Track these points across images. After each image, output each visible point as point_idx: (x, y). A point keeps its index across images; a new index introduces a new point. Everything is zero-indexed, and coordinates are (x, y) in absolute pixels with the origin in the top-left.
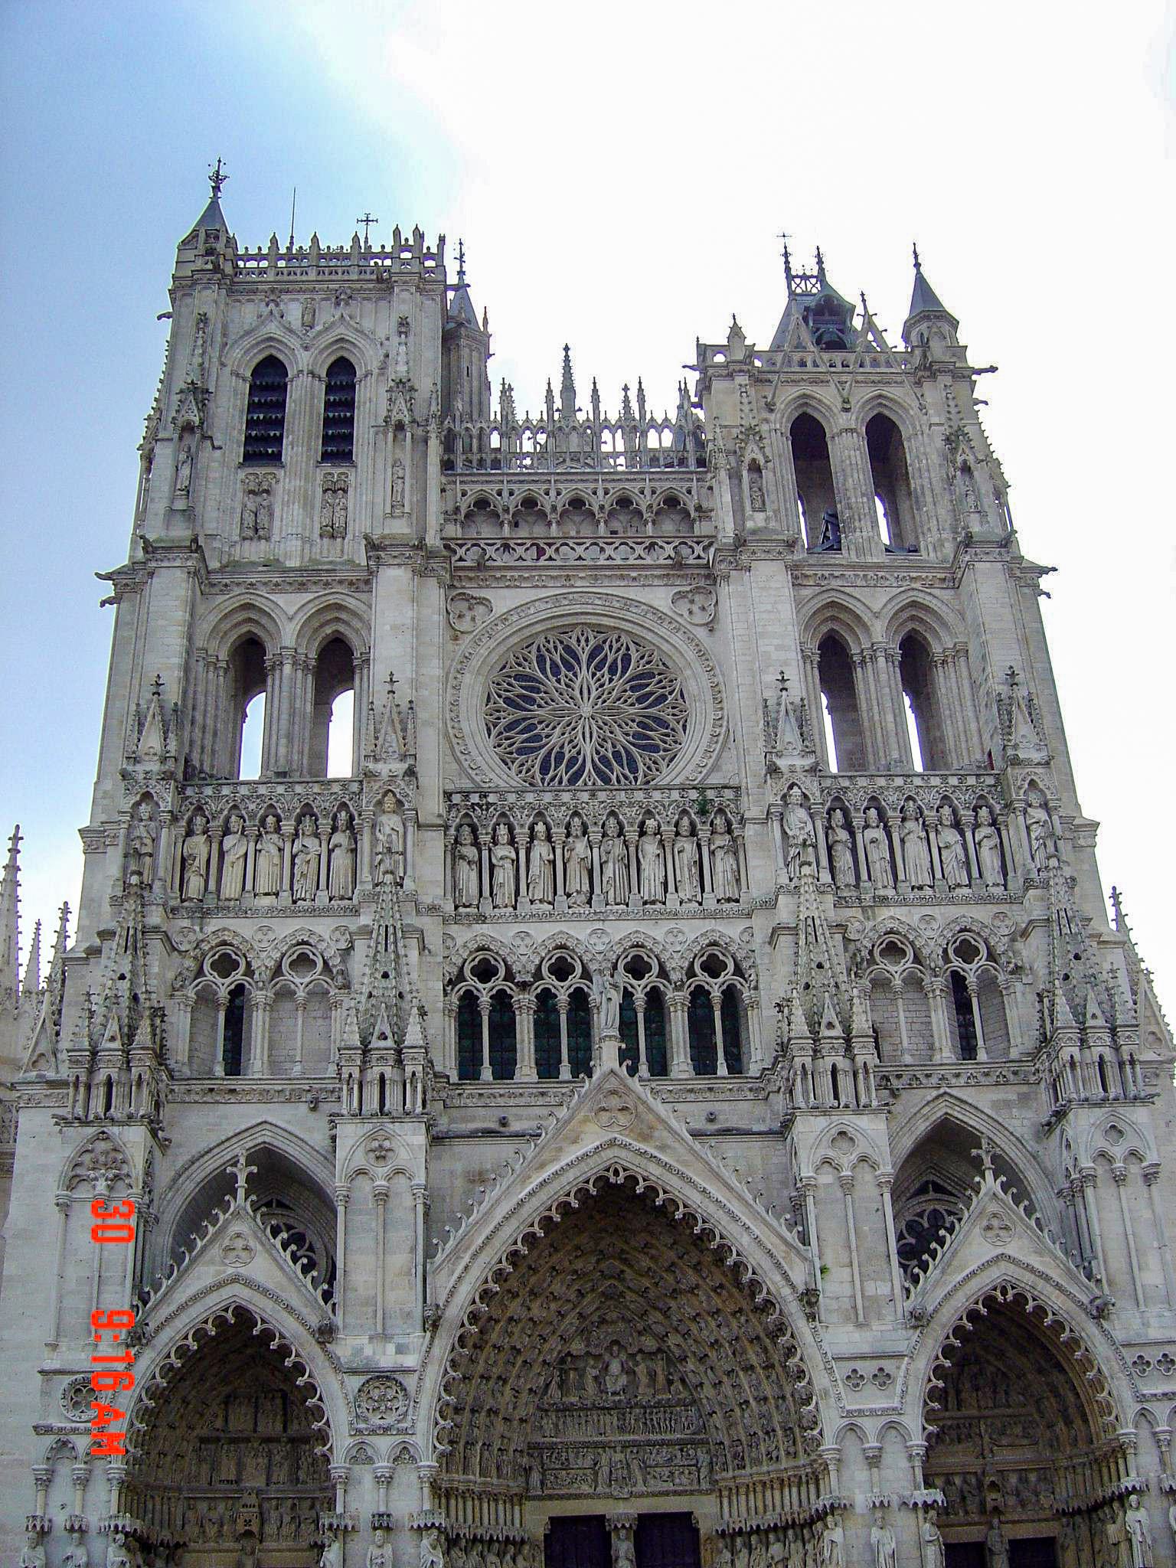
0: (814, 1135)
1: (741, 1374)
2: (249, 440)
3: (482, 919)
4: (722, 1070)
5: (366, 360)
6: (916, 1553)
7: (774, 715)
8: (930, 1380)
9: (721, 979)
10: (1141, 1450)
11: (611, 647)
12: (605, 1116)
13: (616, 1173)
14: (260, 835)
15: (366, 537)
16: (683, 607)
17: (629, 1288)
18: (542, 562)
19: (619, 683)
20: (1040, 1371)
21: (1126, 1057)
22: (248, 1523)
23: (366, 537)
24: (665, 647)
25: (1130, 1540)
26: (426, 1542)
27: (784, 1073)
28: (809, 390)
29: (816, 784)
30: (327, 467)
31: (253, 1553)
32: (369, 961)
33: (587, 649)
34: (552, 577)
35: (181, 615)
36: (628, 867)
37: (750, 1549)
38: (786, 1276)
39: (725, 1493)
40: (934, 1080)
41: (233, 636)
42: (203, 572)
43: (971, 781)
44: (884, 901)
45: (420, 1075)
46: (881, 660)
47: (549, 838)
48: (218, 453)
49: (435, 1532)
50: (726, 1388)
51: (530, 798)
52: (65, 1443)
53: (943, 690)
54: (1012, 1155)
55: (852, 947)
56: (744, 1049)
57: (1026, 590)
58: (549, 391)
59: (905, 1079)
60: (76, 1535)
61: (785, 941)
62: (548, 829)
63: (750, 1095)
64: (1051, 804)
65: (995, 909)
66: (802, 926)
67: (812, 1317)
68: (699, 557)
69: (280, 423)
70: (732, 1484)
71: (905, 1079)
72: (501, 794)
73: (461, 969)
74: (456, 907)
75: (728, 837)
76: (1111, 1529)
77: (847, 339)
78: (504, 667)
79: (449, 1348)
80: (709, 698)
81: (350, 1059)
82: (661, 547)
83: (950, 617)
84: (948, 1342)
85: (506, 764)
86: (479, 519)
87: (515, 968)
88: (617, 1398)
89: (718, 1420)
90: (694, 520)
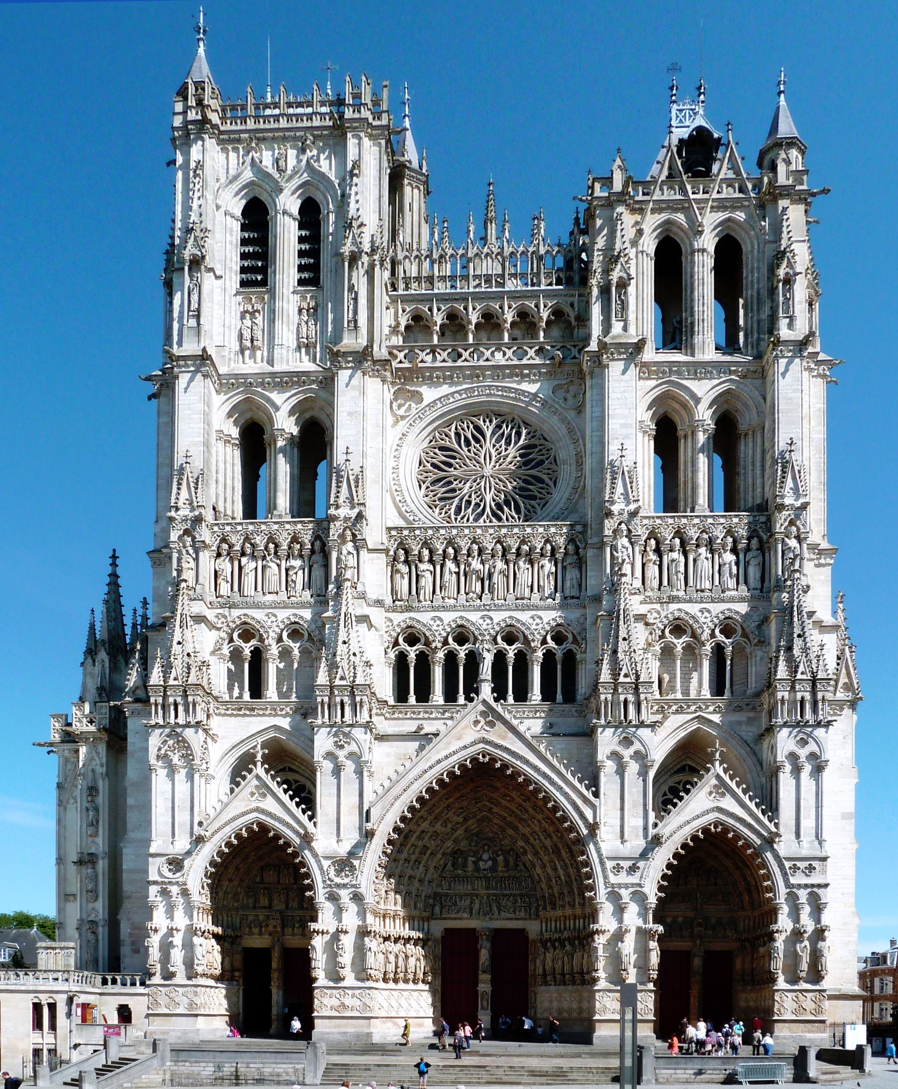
3: (409, 609)
14: (265, 556)
18: (459, 363)
29: (638, 522)
33: (491, 428)
36: (508, 577)
40: (693, 708)
44: (673, 599)
51: (442, 532)
52: (165, 889)
53: (742, 455)
59: (674, 708)
62: (456, 551)
68: (574, 357)
72: (426, 529)
74: (394, 601)
75: (575, 557)
76: (762, 950)
78: (431, 441)
80: (573, 462)
85: (431, 508)
86: (416, 330)
87: (431, 639)
90: (574, 328)
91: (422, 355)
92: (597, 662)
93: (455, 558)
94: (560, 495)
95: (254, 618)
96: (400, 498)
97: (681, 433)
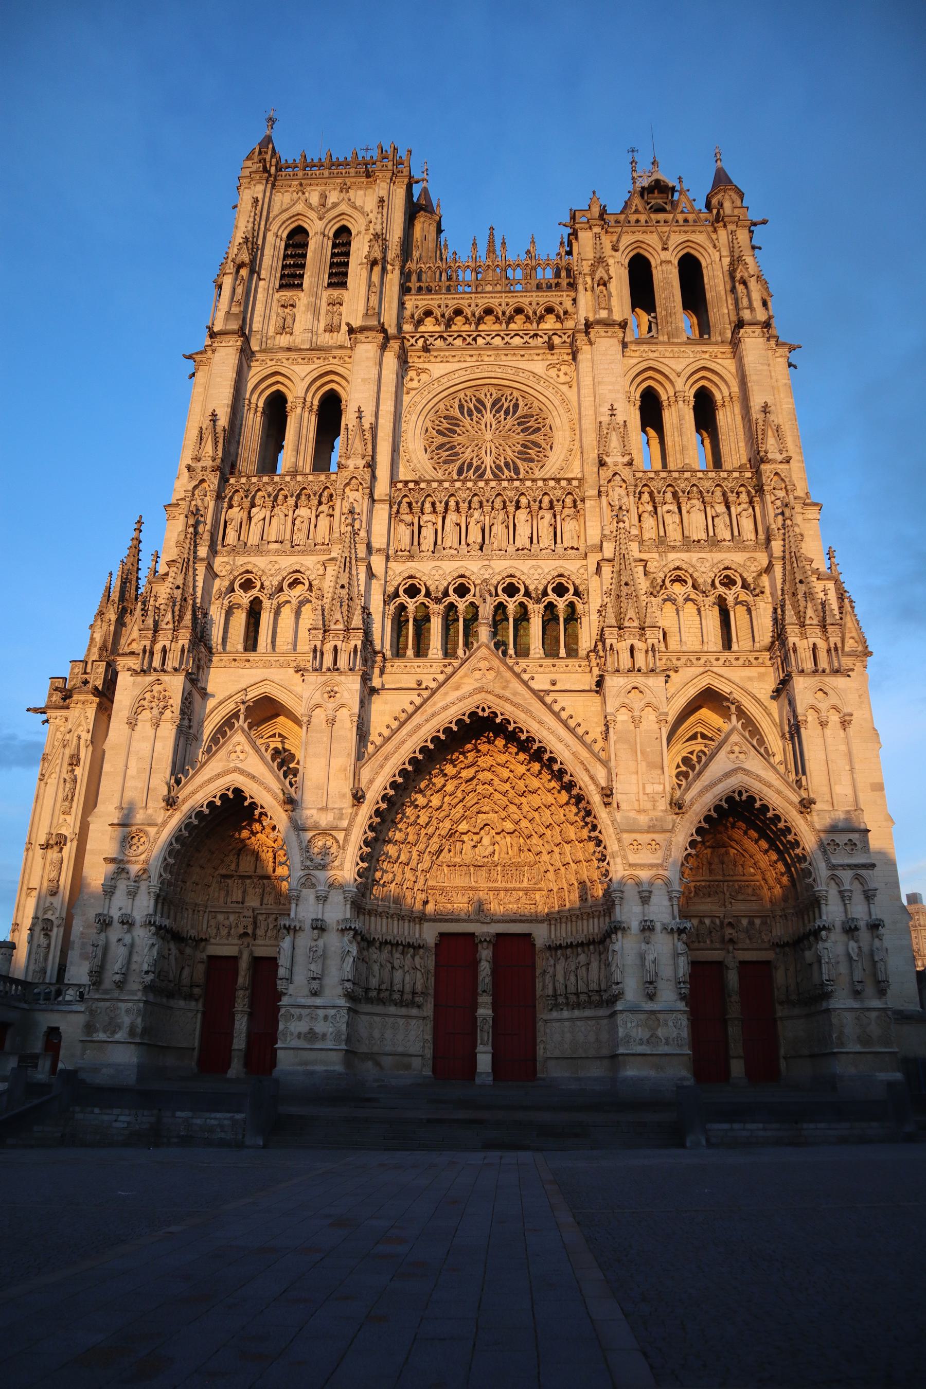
0: (616, 689)
1: (565, 845)
2: (283, 277)
3: (411, 557)
4: (563, 653)
5: (356, 226)
6: (671, 962)
7: (605, 432)
8: (686, 849)
9: (565, 598)
10: (829, 903)
11: (506, 399)
12: (477, 674)
13: (483, 710)
14: (273, 507)
15: (348, 324)
16: (553, 372)
17: (495, 790)
19: (510, 421)
20: (766, 852)
21: (832, 646)
22: (245, 927)
23: (348, 324)
24: (541, 398)
25: (820, 962)
26: (346, 939)
27: (601, 653)
28: (640, 237)
30: (331, 291)
31: (248, 946)
32: (333, 579)
34: (471, 356)
35: (231, 375)
36: (507, 527)
37: (567, 958)
38: (592, 777)
39: (553, 922)
40: (702, 661)
41: (268, 392)
42: (249, 352)
43: (736, 475)
45: (359, 647)
46: (681, 403)
47: (458, 510)
48: (262, 283)
49: (352, 933)
50: (556, 855)
52: (123, 869)
54: (752, 711)
55: (652, 576)
56: (580, 645)
57: (780, 359)
58: (475, 244)
59: (683, 661)
60: (125, 926)
61: (606, 570)
62: (457, 503)
63: (580, 670)
64: (789, 487)
65: (748, 555)
66: (617, 559)
67: (607, 804)
69: (303, 266)
70: (557, 916)
71: (683, 661)
72: (429, 482)
73: (397, 589)
77: (668, 207)
79: (368, 816)
80: (567, 427)
81: (316, 636)
82: (541, 337)
83: (728, 377)
84: (700, 825)
85: (435, 469)
88: (486, 860)
89: (551, 875)
91: (431, 340)
92: (599, 611)
93: (458, 510)
94: (556, 457)
95: (255, 565)
96: (408, 457)
97: (665, 404)
